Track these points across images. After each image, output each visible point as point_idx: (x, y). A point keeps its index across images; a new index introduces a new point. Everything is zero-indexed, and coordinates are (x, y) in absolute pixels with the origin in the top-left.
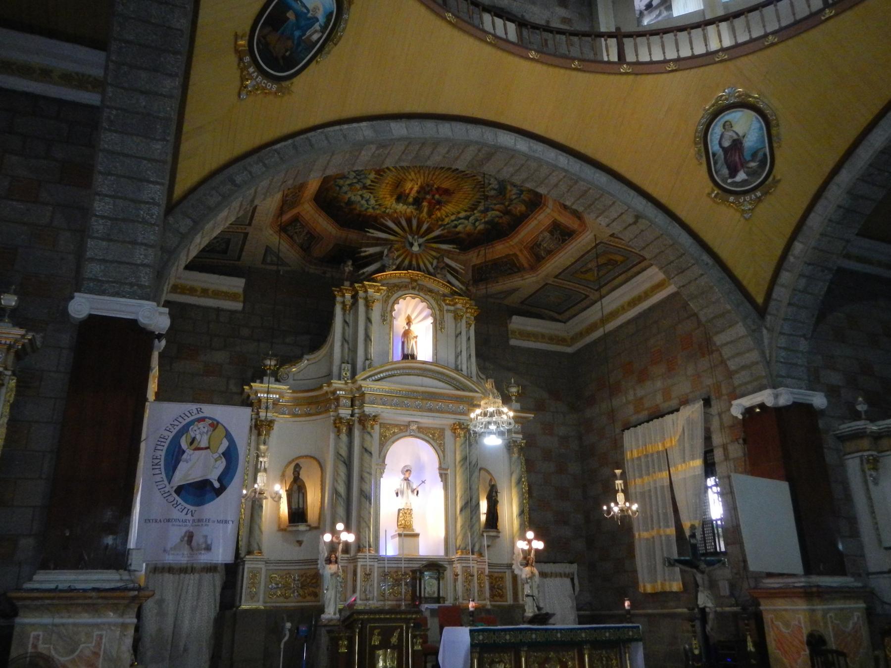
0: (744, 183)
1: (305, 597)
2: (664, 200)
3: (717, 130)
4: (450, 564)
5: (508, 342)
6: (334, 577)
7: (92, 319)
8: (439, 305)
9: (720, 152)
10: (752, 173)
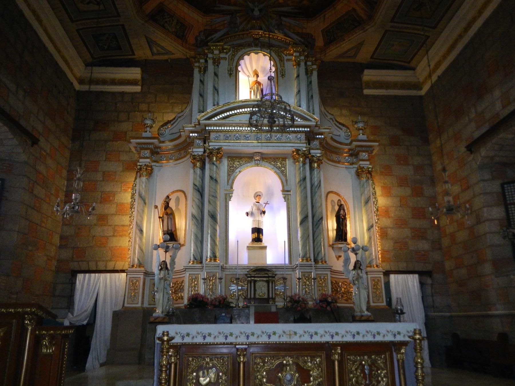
1: (177, 300)
4: (293, 271)
5: (362, 92)
6: (162, 281)
8: (279, 56)
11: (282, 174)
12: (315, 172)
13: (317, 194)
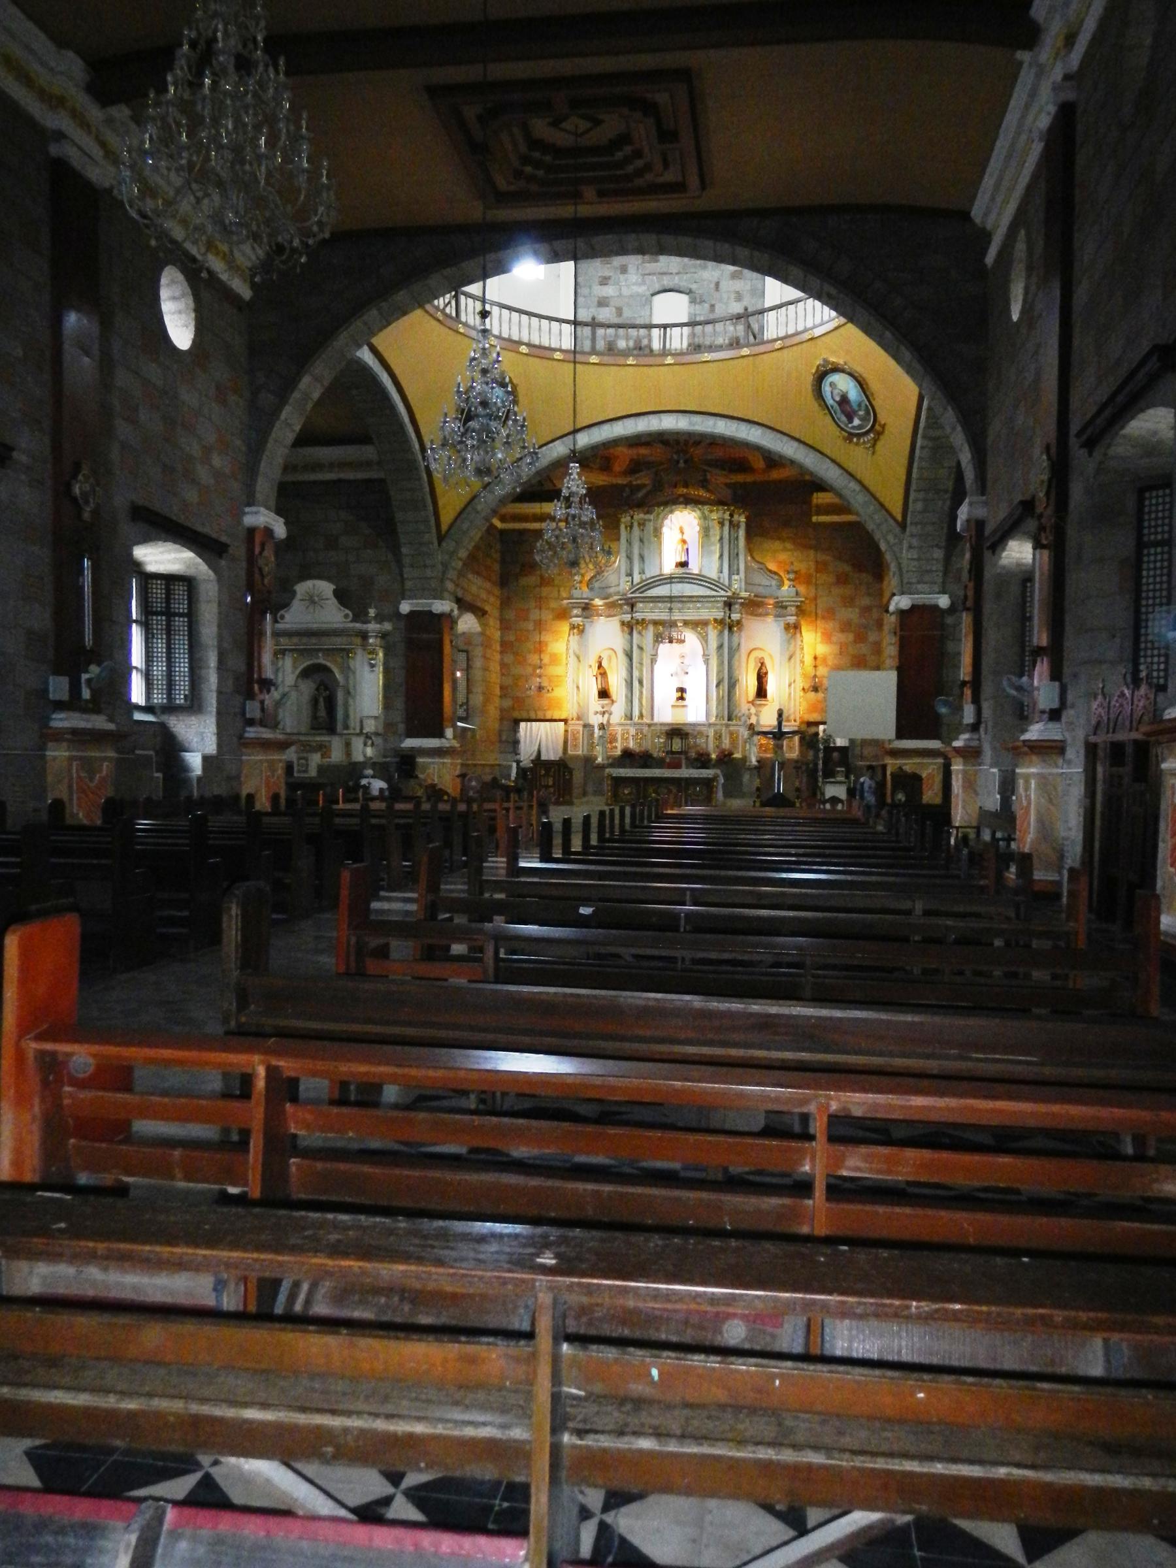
0: (859, 427)
2: (810, 442)
3: (826, 389)
7: (412, 613)
8: (703, 513)
9: (835, 405)
10: (864, 419)
11: (704, 639)
12: (736, 635)
13: (736, 657)
